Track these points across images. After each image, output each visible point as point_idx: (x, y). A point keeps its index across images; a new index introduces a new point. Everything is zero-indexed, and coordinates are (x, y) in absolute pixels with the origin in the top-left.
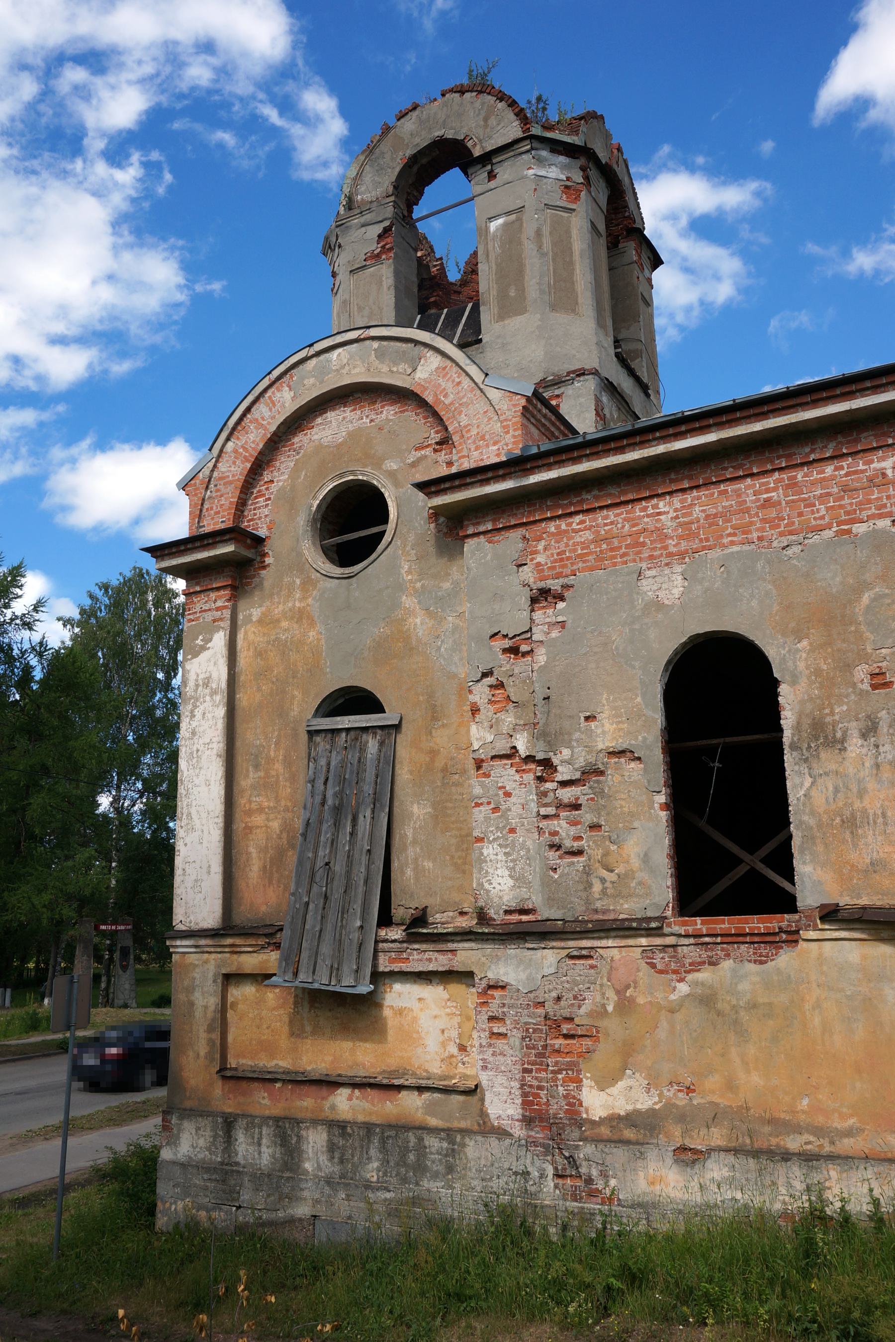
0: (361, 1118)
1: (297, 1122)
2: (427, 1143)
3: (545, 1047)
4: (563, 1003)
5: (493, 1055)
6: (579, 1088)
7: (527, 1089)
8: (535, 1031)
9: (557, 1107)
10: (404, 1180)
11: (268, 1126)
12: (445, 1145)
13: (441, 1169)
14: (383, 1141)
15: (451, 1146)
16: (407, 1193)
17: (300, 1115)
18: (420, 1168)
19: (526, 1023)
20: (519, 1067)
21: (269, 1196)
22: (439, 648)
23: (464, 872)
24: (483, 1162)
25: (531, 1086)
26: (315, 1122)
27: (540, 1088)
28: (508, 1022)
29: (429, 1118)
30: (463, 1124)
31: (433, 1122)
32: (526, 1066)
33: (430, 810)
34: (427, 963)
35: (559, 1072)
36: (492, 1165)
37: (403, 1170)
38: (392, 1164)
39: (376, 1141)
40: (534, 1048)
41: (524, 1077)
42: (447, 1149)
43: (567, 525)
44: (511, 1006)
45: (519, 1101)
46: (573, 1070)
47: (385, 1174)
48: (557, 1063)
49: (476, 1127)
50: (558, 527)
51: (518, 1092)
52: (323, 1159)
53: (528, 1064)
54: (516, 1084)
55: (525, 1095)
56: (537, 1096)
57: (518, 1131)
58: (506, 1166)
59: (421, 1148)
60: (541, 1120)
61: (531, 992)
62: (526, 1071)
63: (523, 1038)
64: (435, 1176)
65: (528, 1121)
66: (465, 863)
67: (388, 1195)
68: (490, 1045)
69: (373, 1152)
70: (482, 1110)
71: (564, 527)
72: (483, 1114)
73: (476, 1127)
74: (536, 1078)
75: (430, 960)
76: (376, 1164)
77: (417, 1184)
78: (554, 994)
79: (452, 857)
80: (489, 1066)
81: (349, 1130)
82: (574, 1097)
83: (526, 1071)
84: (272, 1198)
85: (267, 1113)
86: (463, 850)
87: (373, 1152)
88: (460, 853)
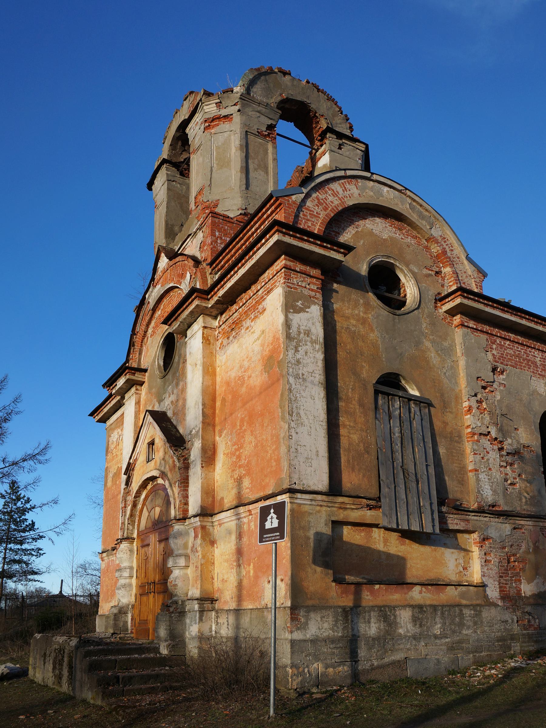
0: (428, 602)
1: (393, 608)
2: (464, 612)
3: (507, 566)
4: (513, 547)
5: (487, 570)
6: (521, 584)
7: (501, 585)
8: (503, 560)
9: (513, 592)
10: (454, 632)
11: (374, 611)
12: (472, 612)
13: (471, 624)
14: (442, 613)
15: (475, 612)
16: (456, 638)
17: (393, 604)
18: (461, 625)
19: (500, 556)
20: (498, 575)
21: (378, 651)
22: (445, 373)
23: (462, 485)
24: (489, 618)
25: (503, 583)
26: (404, 607)
27: (506, 584)
28: (492, 555)
29: (462, 600)
30: (478, 602)
31: (464, 602)
32: (500, 575)
33: (445, 451)
34: (455, 526)
35: (513, 577)
36: (493, 619)
37: (453, 627)
38: (447, 624)
39: (439, 613)
40: (503, 567)
41: (500, 579)
42: (473, 614)
43: (504, 343)
44: (494, 548)
45: (498, 590)
46: (518, 576)
47: (444, 630)
48: (512, 573)
49: (483, 603)
50: (501, 342)
51: (498, 586)
52: (410, 626)
53: (502, 573)
54: (497, 583)
55: (500, 587)
56: (506, 587)
57: (500, 603)
58: (499, 619)
59: (461, 614)
60: (508, 598)
61: (501, 542)
62: (501, 577)
63: (499, 562)
64: (468, 628)
65: (503, 598)
66: (463, 481)
67: (447, 640)
68: (486, 565)
69: (438, 619)
70: (485, 595)
71: (502, 343)
72: (486, 597)
73: (483, 603)
74: (505, 580)
75: (457, 524)
76: (439, 626)
77: (460, 633)
78: (510, 543)
79: (457, 477)
80: (486, 575)
81: (425, 609)
82: (519, 588)
83: (501, 577)
84: (380, 652)
85: (371, 604)
86: (461, 474)
87: (438, 619)
88: (460, 475)
